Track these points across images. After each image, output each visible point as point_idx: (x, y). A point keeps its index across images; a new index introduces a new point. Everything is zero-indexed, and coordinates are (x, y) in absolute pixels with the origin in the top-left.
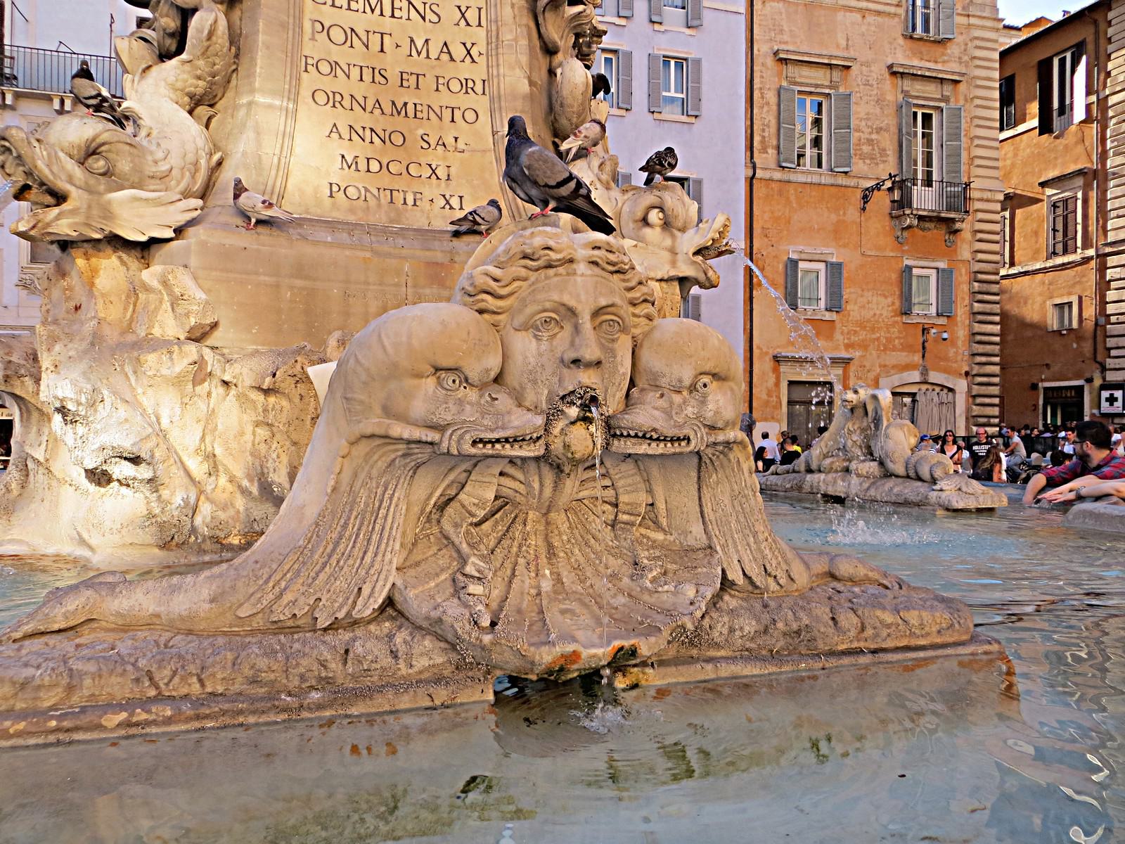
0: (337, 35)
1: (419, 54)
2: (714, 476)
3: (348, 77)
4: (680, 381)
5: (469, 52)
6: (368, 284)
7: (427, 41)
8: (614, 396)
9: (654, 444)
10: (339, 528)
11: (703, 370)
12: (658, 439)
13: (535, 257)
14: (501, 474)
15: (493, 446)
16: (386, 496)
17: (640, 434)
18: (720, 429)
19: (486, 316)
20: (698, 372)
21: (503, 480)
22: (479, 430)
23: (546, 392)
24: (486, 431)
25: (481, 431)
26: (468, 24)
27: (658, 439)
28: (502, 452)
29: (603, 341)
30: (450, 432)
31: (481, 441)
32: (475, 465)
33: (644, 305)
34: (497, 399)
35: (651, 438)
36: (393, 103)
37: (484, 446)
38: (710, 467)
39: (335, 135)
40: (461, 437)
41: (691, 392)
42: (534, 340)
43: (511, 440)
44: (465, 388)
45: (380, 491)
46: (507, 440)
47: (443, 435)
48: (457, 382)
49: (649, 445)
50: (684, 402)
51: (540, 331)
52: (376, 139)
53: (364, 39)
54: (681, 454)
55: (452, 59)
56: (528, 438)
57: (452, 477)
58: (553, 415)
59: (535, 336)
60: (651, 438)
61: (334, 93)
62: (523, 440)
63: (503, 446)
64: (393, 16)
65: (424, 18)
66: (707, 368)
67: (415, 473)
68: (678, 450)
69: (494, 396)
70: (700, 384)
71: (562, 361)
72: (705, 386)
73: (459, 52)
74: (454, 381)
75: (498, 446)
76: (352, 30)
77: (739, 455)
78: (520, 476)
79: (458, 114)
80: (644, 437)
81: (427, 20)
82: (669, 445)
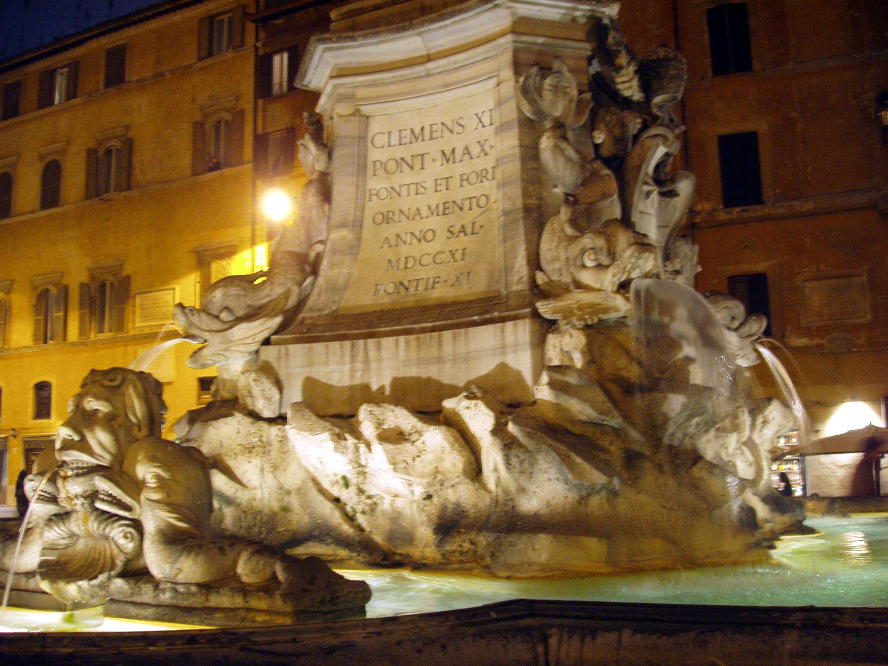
0: (392, 166)
1: (448, 161)
3: (399, 195)
5: (483, 150)
7: (453, 151)
26: (484, 126)
36: (429, 207)
39: (386, 246)
52: (415, 241)
53: (410, 162)
55: (471, 158)
61: (388, 212)
64: (431, 139)
65: (452, 132)
73: (475, 150)
76: (402, 159)
79: (474, 201)
81: (455, 131)
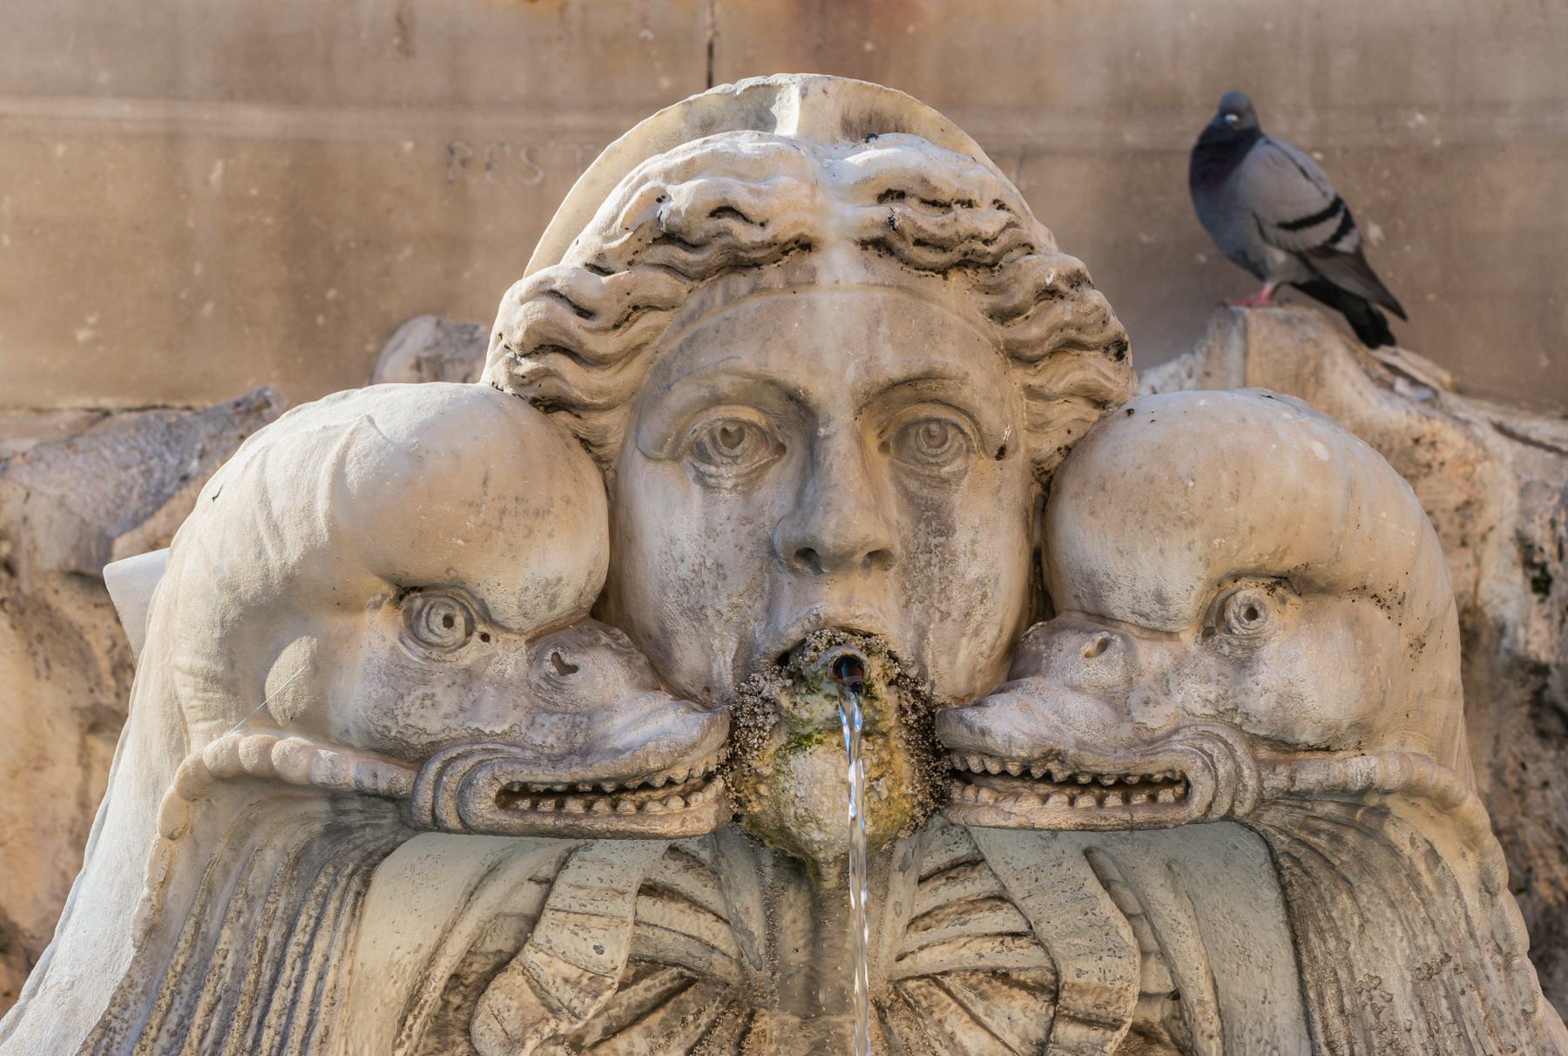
2: (1344, 900)
4: (1161, 599)
6: (548, 106)
8: (952, 651)
9: (1058, 800)
10: (164, 1040)
11: (1236, 564)
12: (1071, 781)
13: (696, 237)
14: (649, 890)
15: (560, 806)
16: (293, 950)
17: (1014, 769)
18: (1311, 749)
19: (563, 417)
20: (1221, 568)
21: (653, 910)
22: (515, 760)
23: (732, 645)
24: (536, 762)
25: (525, 762)
27: (1071, 781)
28: (584, 823)
29: (913, 485)
30: (435, 766)
31: (525, 791)
32: (563, 864)
33: (1069, 360)
34: (573, 669)
35: (1047, 777)
37: (534, 806)
38: (1312, 863)
40: (468, 782)
41: (1208, 633)
42: (696, 489)
43: (609, 787)
44: (485, 638)
45: (274, 938)
46: (597, 790)
47: (419, 776)
48: (460, 620)
49: (1045, 799)
50: (1178, 667)
51: (708, 460)
54: (1159, 826)
56: (659, 781)
57: (492, 896)
58: (753, 714)
59: (701, 478)
60: (1047, 777)
62: (646, 786)
63: (589, 807)
66: (1248, 557)
67: (366, 883)
68: (1141, 816)
69: (568, 660)
70: (1234, 611)
71: (773, 552)
72: (1252, 614)
74: (449, 622)
75: (575, 806)
77: (1431, 832)
78: (706, 893)
80: (1025, 774)
82: (1113, 800)
